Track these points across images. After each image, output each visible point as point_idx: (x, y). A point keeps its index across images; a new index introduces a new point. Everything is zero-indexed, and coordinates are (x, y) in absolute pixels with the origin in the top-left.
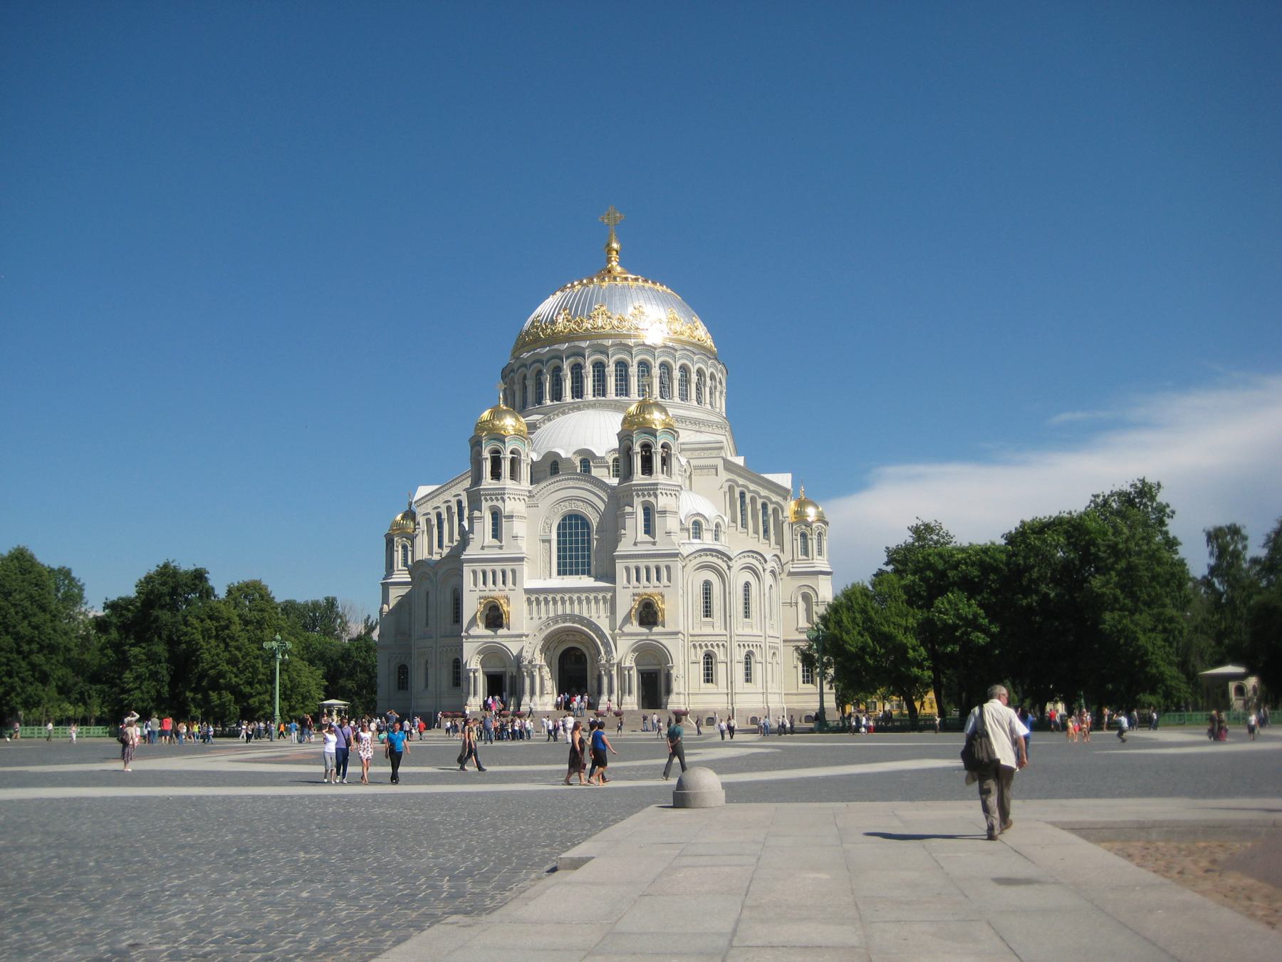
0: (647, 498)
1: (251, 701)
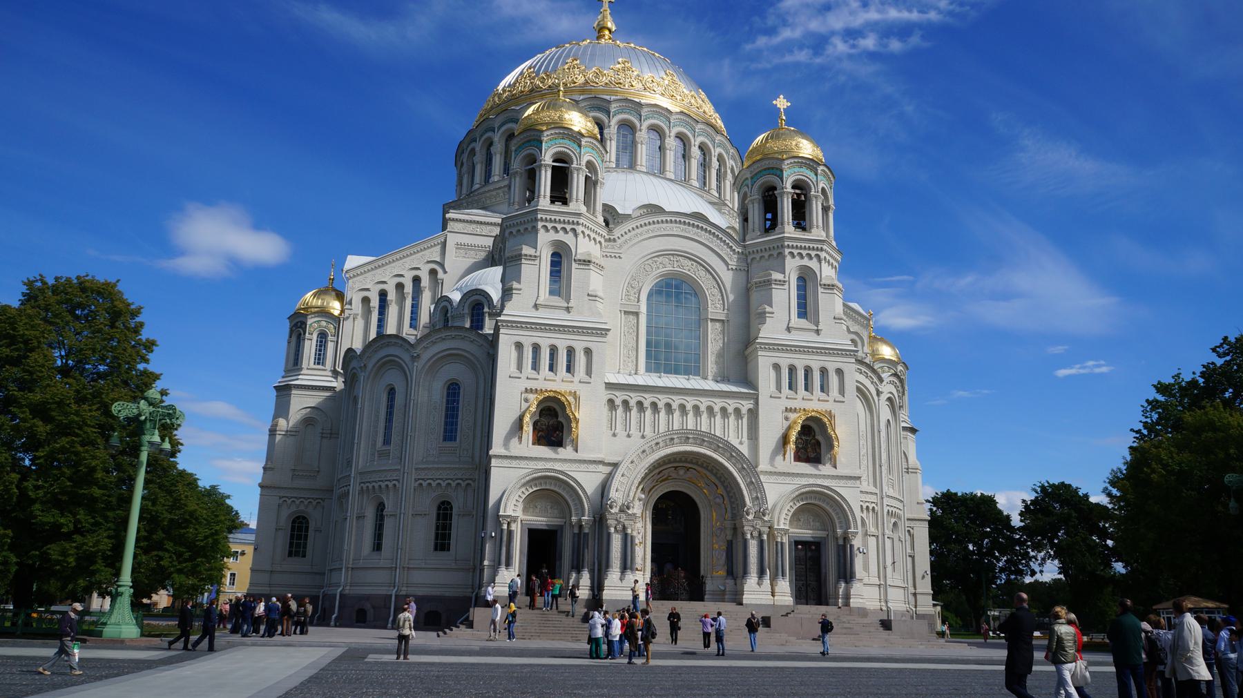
0: (806, 262)
1: (54, 551)
